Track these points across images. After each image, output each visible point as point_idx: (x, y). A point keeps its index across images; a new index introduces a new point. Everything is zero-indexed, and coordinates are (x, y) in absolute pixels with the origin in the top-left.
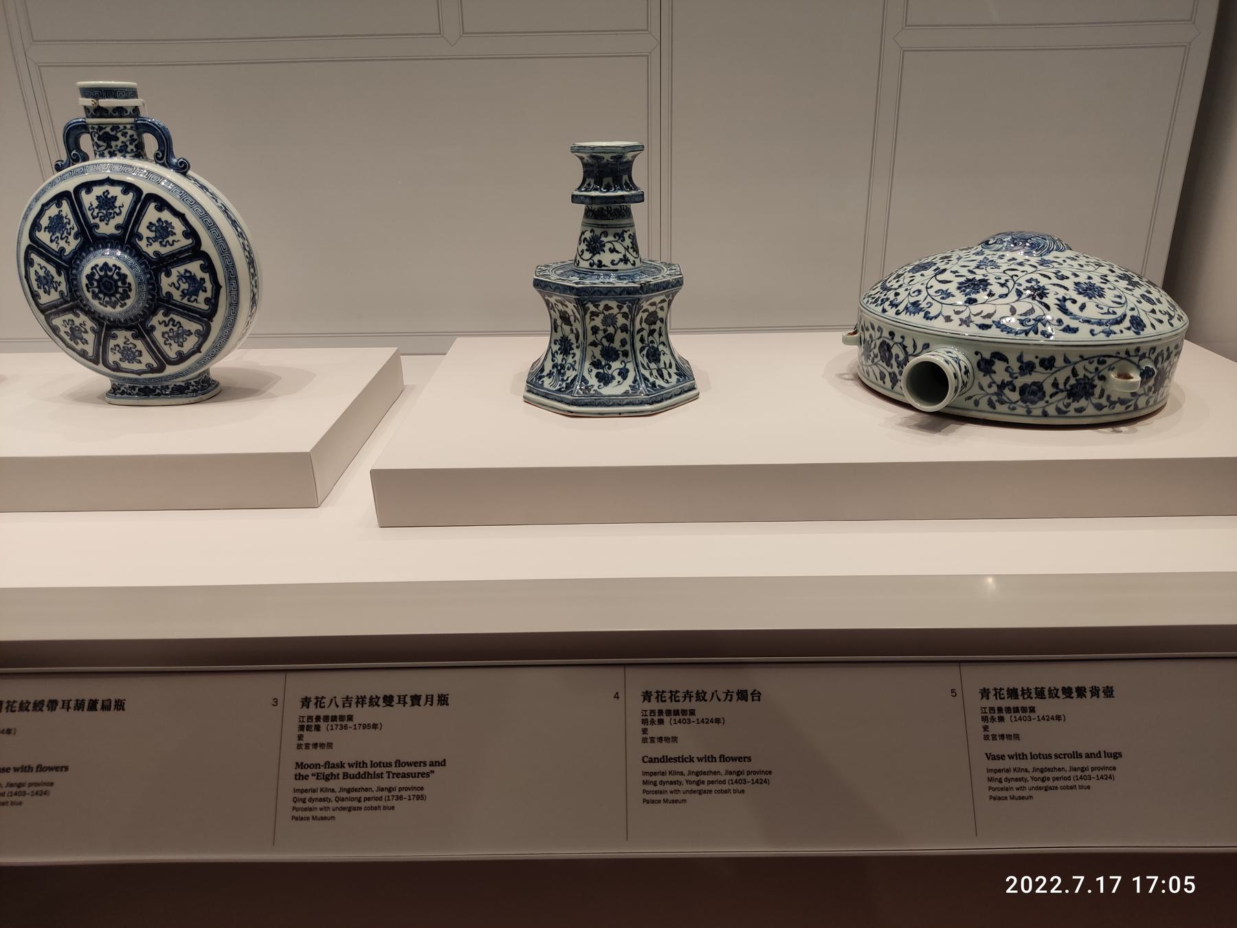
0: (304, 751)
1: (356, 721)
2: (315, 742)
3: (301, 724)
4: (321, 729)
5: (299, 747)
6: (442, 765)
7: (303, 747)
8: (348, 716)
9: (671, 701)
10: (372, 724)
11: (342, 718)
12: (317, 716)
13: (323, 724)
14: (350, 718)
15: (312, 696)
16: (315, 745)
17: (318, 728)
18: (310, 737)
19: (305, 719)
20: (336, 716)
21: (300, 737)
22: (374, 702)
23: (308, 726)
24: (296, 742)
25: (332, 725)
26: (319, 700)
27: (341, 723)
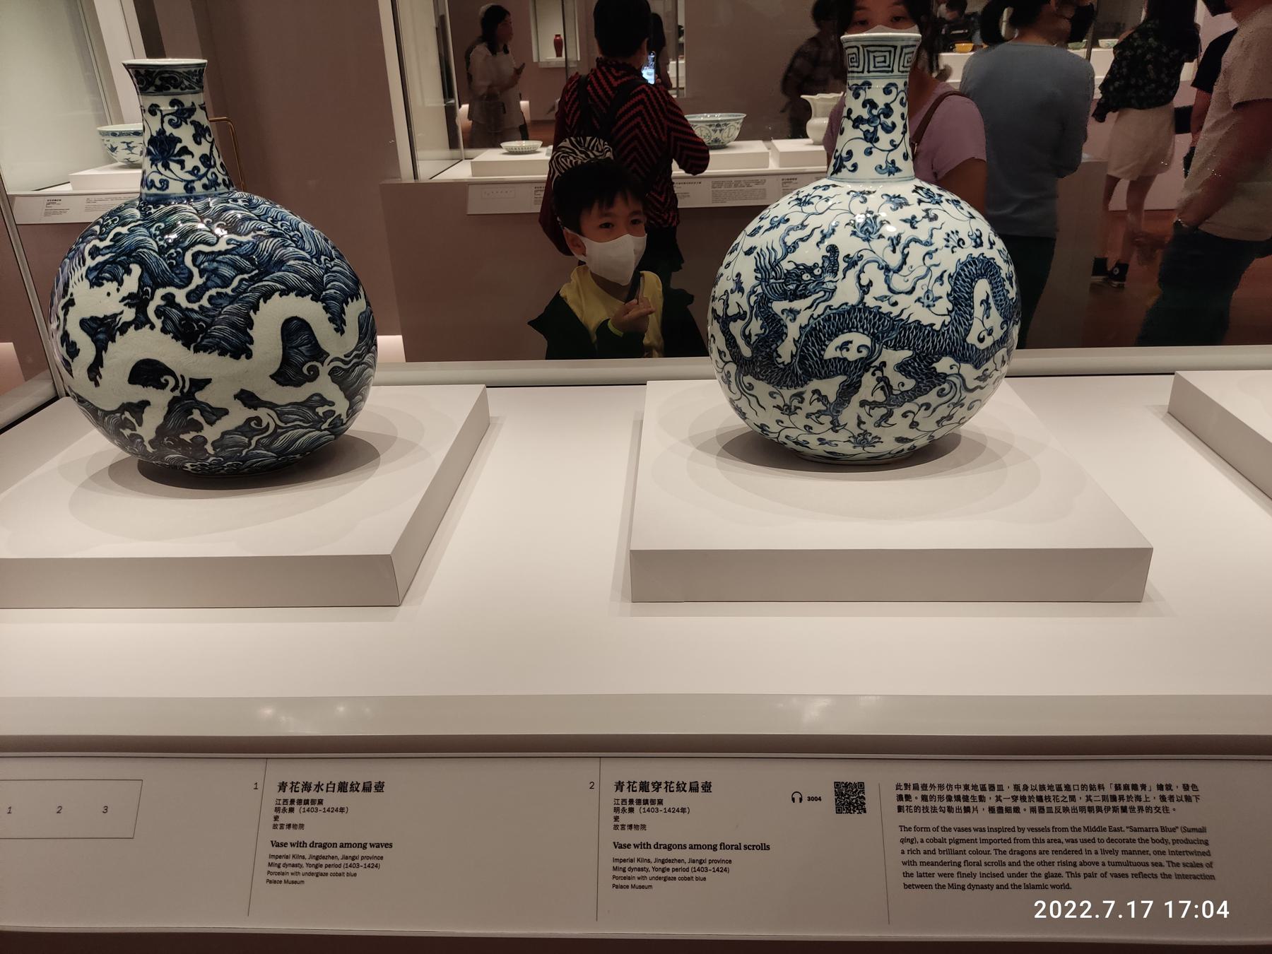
0: (278, 831)
1: (326, 805)
3: (278, 806)
4: (295, 812)
5: (275, 827)
11: (313, 802)
13: (296, 807)
14: (321, 802)
15: (289, 781)
17: (292, 810)
18: (285, 818)
19: (281, 802)
20: (308, 800)
21: (276, 818)
22: (343, 787)
27: (313, 806)
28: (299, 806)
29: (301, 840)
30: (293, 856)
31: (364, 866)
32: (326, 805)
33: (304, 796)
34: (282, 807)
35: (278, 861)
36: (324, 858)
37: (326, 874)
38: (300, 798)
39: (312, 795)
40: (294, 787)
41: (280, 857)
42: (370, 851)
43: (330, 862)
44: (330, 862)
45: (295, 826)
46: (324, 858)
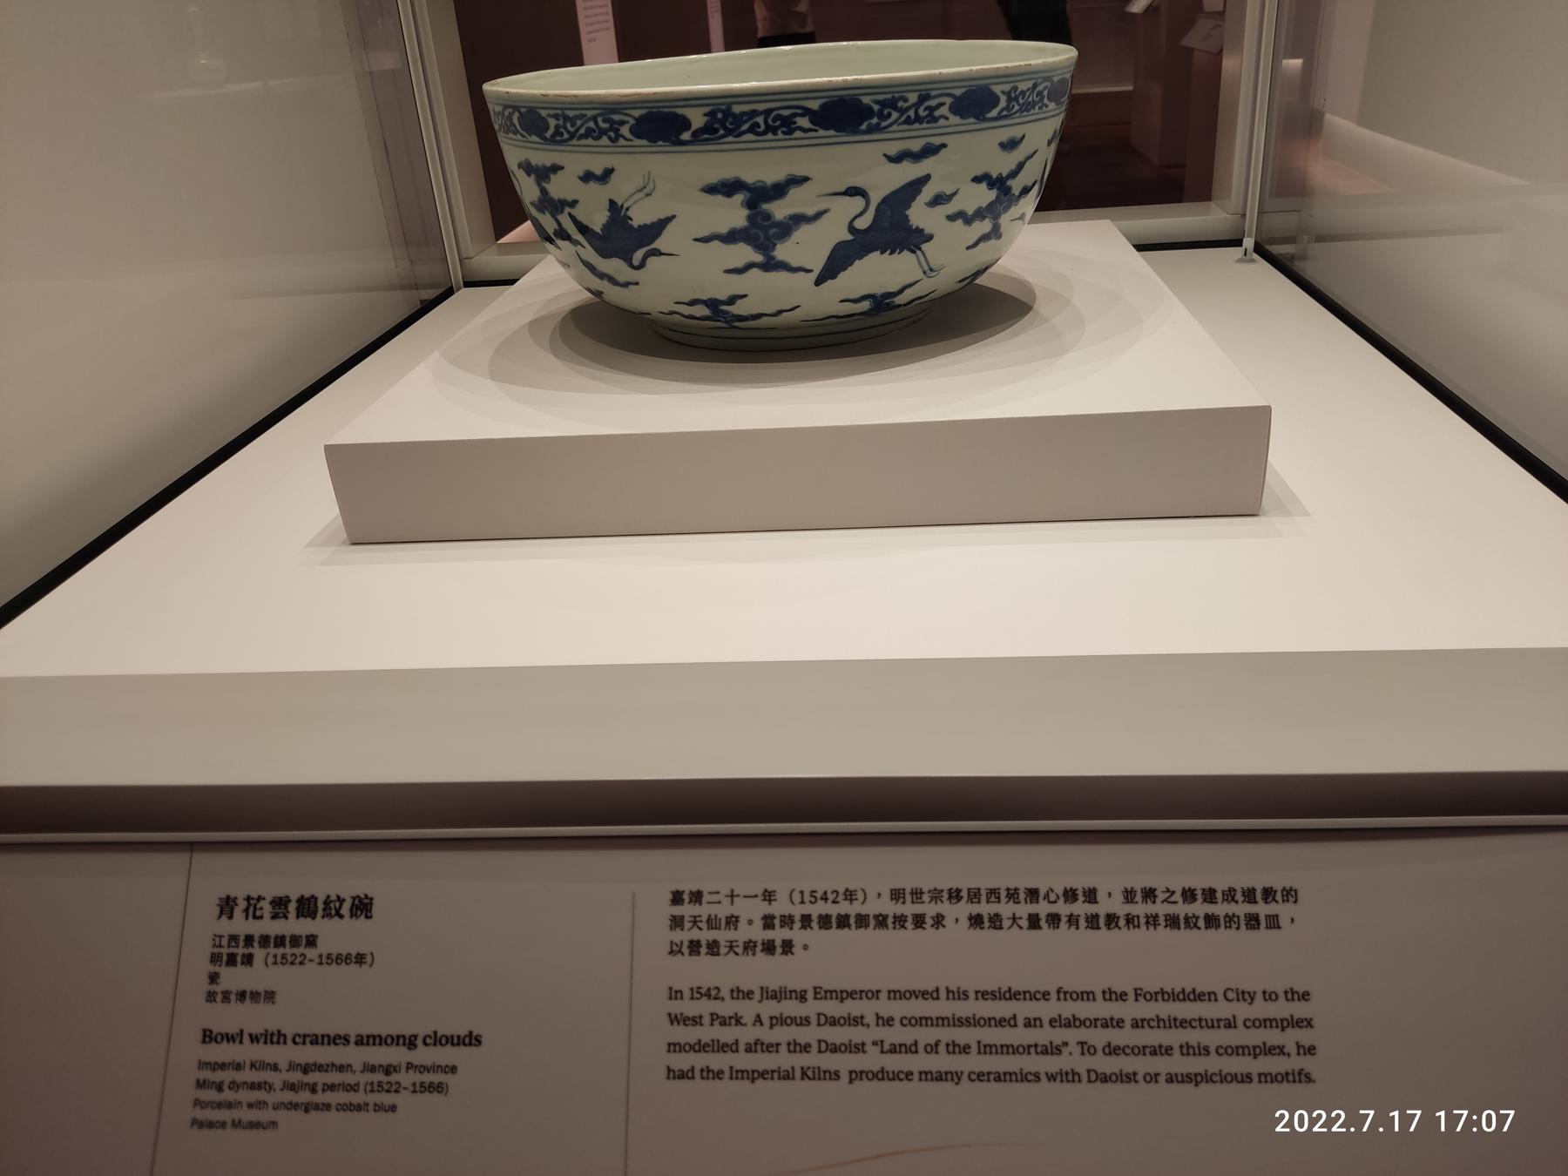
0: (218, 1006)
2: (241, 990)
3: (216, 950)
7: (219, 997)
8: (307, 936)
10: (354, 954)
11: (295, 940)
12: (246, 936)
13: (258, 953)
14: (312, 941)
16: (242, 996)
17: (248, 960)
18: (233, 978)
19: (225, 942)
20: (283, 937)
21: (214, 978)
23: (228, 955)
24: (205, 986)
26: (252, 902)
27: (295, 950)
29: (272, 1028)
30: (253, 1065)
35: (218, 1076)
36: (320, 1068)
38: (264, 933)
39: (294, 926)
40: (252, 907)
41: (223, 1066)
42: (424, 1055)
43: (334, 1077)
44: (334, 1077)
45: (255, 996)
46: (320, 1068)
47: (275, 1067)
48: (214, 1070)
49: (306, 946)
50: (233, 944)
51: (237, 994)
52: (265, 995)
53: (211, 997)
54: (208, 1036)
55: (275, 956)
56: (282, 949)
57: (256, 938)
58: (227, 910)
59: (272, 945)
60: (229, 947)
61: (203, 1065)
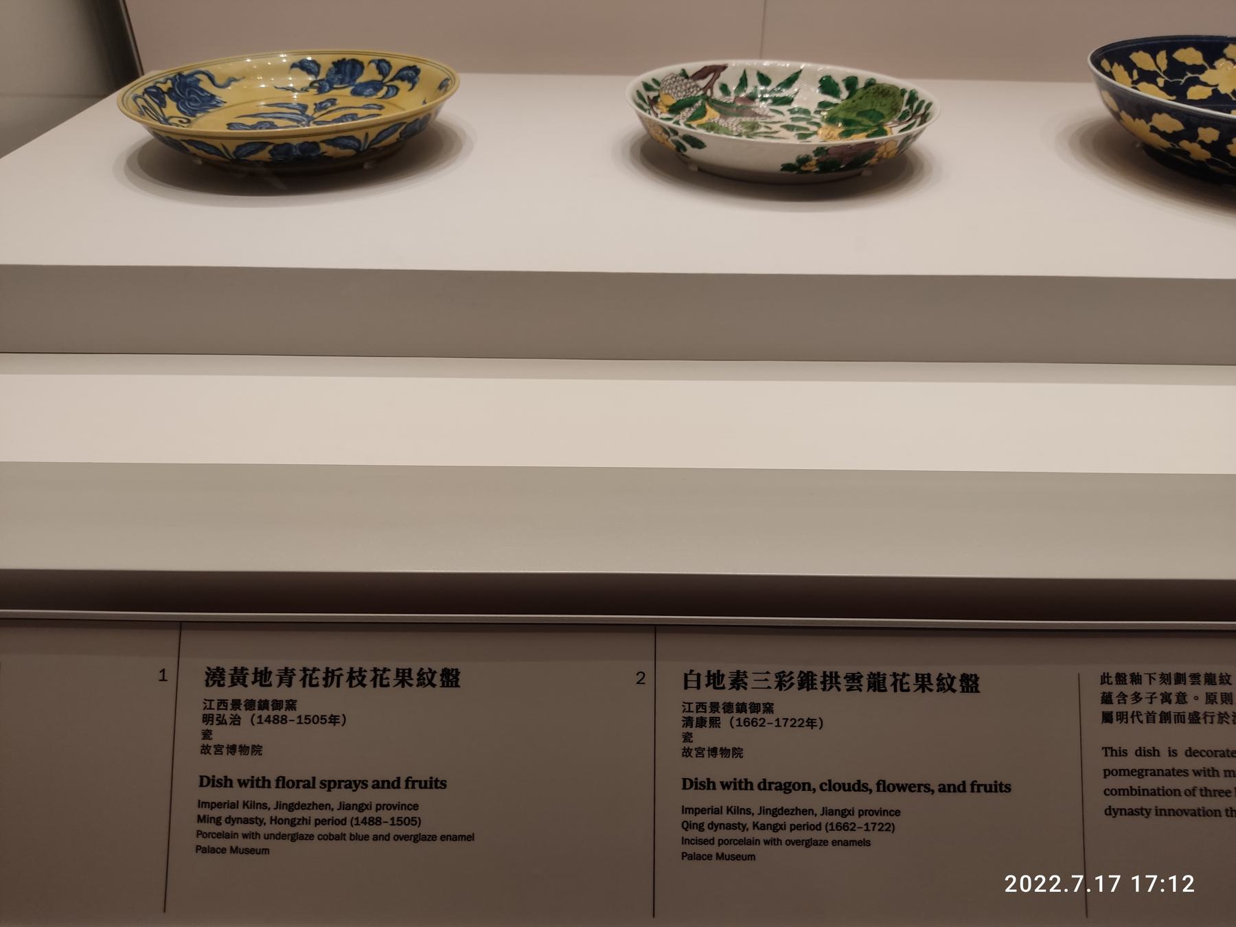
0: (212, 758)
1: (302, 710)
4: (242, 721)
5: (205, 750)
6: (334, 781)
7: (212, 750)
9: (895, 691)
11: (277, 705)
13: (244, 714)
14: (291, 705)
16: (232, 749)
17: (236, 721)
18: (223, 735)
19: (214, 705)
20: (266, 702)
21: (207, 734)
25: (260, 717)
27: (277, 712)
28: (250, 713)
31: (391, 822)
32: (302, 710)
33: (255, 692)
34: (215, 712)
37: (311, 837)
40: (239, 676)
45: (244, 749)
47: (264, 806)
48: (212, 808)
49: (286, 709)
50: (222, 707)
51: (228, 748)
52: (252, 748)
53: (205, 750)
54: (208, 781)
55: (260, 717)
56: (265, 710)
57: (242, 702)
58: (286, 679)
59: (256, 708)
60: (218, 709)
61: (201, 804)
